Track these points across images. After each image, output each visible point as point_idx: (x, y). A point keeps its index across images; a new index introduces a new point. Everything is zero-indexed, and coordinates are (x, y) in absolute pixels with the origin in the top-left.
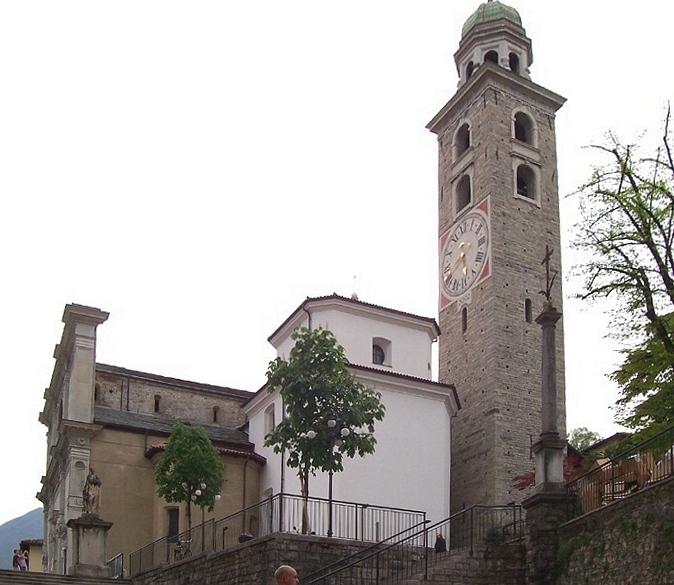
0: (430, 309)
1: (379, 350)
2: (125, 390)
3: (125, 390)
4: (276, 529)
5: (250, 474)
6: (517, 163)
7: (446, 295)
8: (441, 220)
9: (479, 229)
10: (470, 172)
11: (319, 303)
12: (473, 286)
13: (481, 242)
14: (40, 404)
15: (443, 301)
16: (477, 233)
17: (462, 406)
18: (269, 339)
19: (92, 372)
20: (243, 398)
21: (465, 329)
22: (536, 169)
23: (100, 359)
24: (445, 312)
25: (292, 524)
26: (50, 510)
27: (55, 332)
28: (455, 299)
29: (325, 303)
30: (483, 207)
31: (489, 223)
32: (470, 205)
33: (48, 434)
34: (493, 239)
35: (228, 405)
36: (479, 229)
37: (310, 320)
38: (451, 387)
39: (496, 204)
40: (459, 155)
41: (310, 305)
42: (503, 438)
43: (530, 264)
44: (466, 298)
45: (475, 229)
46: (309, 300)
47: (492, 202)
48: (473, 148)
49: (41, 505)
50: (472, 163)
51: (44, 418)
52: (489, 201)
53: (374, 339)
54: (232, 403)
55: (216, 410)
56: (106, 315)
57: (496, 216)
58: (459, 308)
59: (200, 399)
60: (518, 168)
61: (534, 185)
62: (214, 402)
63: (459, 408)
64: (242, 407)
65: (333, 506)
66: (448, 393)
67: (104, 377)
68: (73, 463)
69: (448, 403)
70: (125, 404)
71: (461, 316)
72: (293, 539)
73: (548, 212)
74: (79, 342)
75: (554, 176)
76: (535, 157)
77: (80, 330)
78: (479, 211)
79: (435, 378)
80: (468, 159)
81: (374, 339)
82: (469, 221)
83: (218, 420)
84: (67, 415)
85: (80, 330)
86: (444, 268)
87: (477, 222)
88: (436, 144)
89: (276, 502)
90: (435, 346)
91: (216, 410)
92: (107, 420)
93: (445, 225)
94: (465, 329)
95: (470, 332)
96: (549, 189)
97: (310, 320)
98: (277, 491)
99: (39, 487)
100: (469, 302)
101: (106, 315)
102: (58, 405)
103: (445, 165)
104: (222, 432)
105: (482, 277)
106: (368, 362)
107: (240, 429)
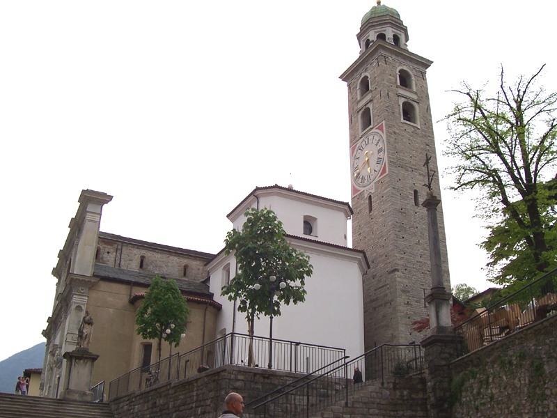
0: (346, 196)
1: (308, 225)
2: (119, 252)
3: (119, 252)
4: (227, 362)
5: (209, 316)
6: (402, 101)
7: (356, 186)
8: (351, 135)
9: (378, 143)
10: (370, 106)
11: (265, 191)
12: (375, 181)
13: (380, 151)
14: (54, 262)
15: (354, 190)
16: (377, 145)
17: (371, 267)
18: (228, 216)
19: (95, 239)
20: (207, 258)
21: (371, 210)
22: (415, 104)
23: (102, 229)
24: (356, 199)
25: (240, 357)
26: (51, 345)
27: (72, 209)
28: (362, 189)
29: (270, 191)
30: (381, 128)
31: (384, 138)
32: (371, 127)
33: (58, 284)
34: (388, 149)
35: (195, 264)
36: (378, 143)
37: (258, 202)
38: (362, 252)
39: (389, 127)
40: (362, 95)
41: (258, 192)
42: (403, 291)
43: (415, 166)
44: (370, 189)
45: (375, 142)
46: (257, 189)
47: (386, 125)
48: (371, 91)
49: (44, 340)
50: (372, 100)
51: (56, 272)
52: (384, 125)
53: (304, 216)
54: (198, 263)
55: (186, 267)
56: (110, 198)
57: (389, 135)
58: (366, 196)
59: (174, 259)
60: (403, 103)
61: (414, 114)
62: (185, 261)
63: (369, 267)
64: (205, 265)
65: (273, 343)
66: (360, 256)
67: (104, 242)
68: (73, 307)
69: (360, 264)
70: (118, 262)
71: (367, 201)
72: (241, 371)
73: (425, 132)
74: (89, 216)
75: (428, 109)
76: (415, 97)
77: (90, 208)
78: (377, 131)
79: (350, 245)
80: (368, 97)
81: (304, 216)
82: (371, 137)
83: (187, 275)
84: (73, 269)
85: (90, 208)
86: (354, 168)
87: (377, 138)
88: (346, 88)
89: (229, 340)
90: (349, 223)
91: (186, 267)
92: (103, 274)
93: (354, 140)
94: (371, 210)
95: (374, 213)
96: (426, 117)
97: (258, 202)
98: (229, 331)
99: (45, 326)
100: (373, 191)
101: (110, 198)
102: (68, 262)
103: (352, 102)
104: (190, 284)
105: (382, 174)
106: (300, 233)
107: (204, 282)
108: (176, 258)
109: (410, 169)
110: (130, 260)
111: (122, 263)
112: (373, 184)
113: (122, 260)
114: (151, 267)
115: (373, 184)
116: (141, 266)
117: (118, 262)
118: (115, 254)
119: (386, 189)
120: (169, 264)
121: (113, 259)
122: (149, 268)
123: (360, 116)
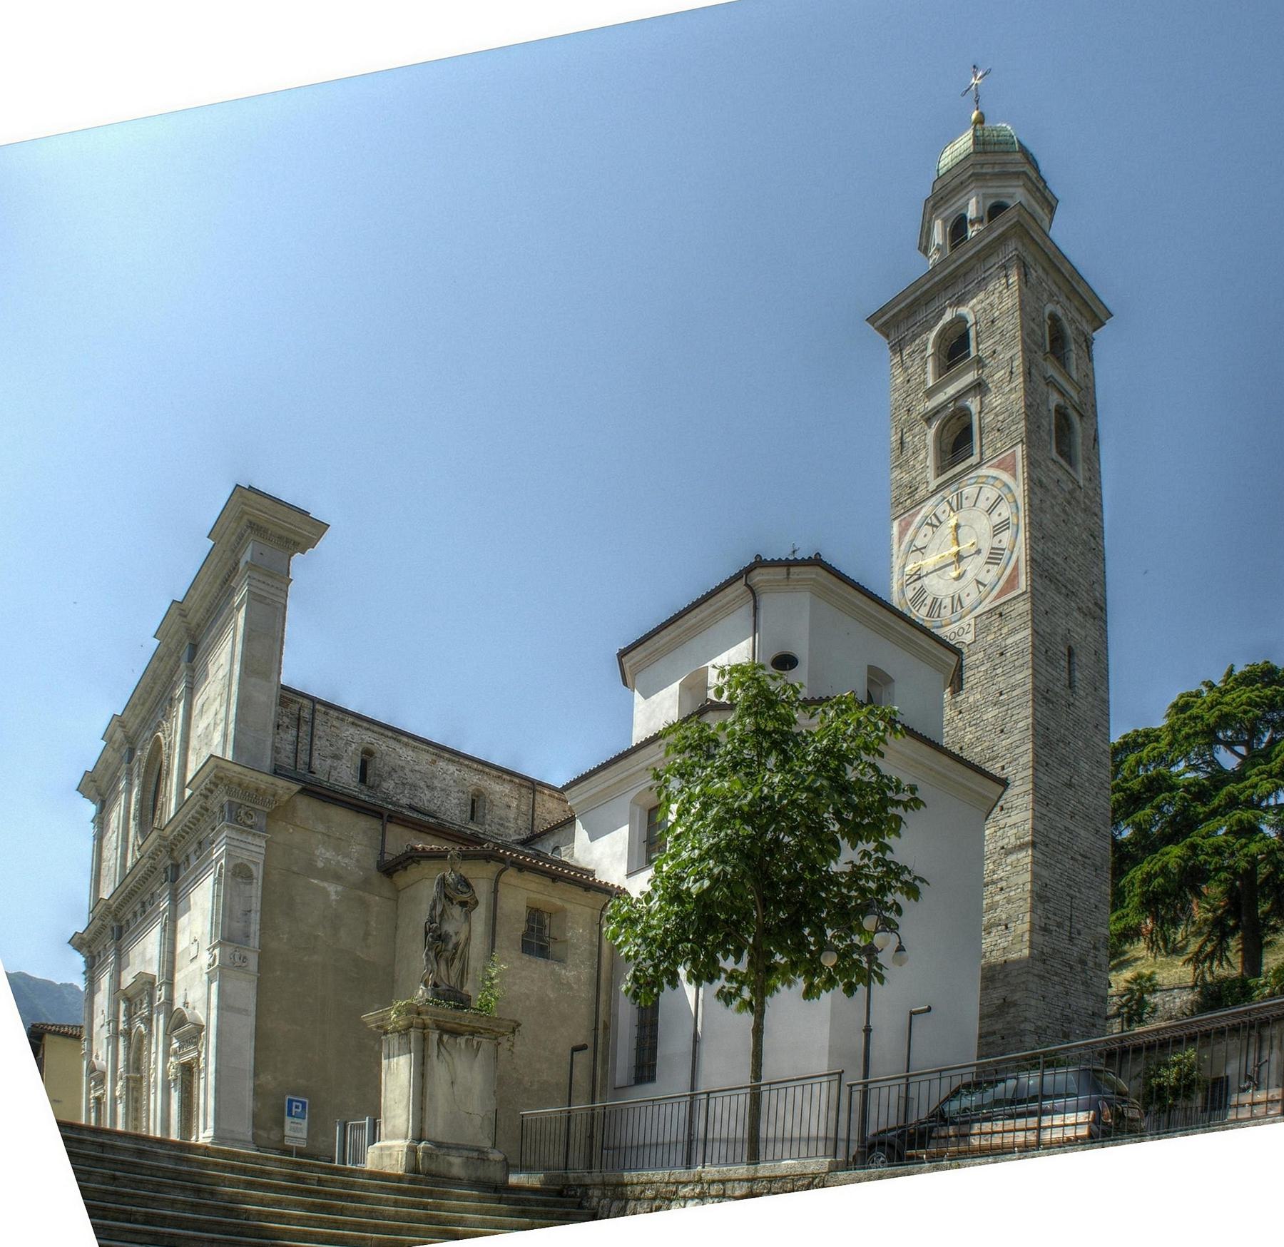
10: (973, 404)
12: (979, 611)
13: (997, 530)
16: (990, 511)
32: (974, 460)
45: (983, 504)
87: (990, 493)
108: (452, 768)
109: (1064, 590)
110: (336, 757)
111: (316, 763)
112: (969, 619)
113: (315, 754)
114: (388, 785)
115: (969, 619)
116: (363, 779)
117: (303, 757)
118: (294, 732)
119: (1013, 632)
120: (436, 783)
121: (289, 748)
122: (385, 785)
123: (932, 432)
